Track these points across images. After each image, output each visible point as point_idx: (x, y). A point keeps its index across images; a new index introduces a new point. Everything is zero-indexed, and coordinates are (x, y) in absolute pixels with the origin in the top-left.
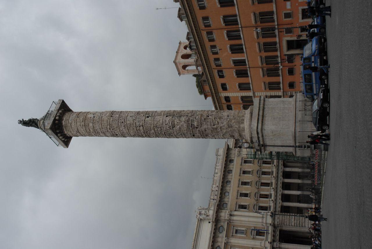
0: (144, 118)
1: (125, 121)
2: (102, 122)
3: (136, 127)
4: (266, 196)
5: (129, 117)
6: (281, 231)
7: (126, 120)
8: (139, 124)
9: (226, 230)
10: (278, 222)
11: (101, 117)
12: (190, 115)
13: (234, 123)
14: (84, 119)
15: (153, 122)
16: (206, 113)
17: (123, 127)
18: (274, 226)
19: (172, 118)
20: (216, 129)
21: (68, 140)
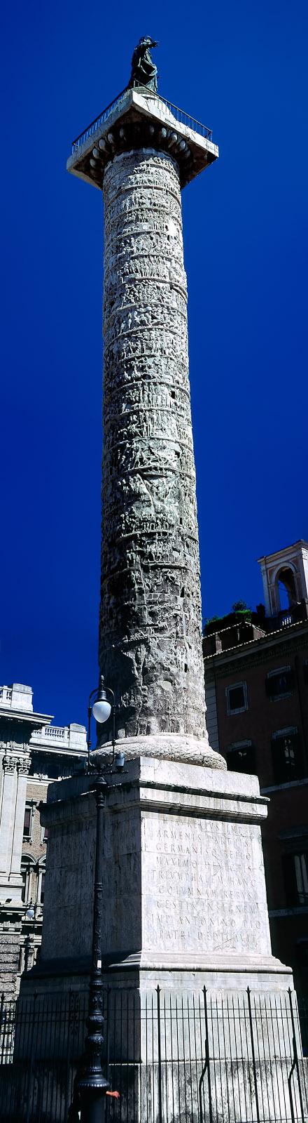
0: (171, 383)
1: (157, 324)
2: (152, 259)
3: (142, 356)
5: (172, 336)
7: (161, 327)
8: (150, 367)
11: (170, 257)
12: (185, 530)
13: (163, 690)
15: (157, 408)
16: (194, 590)
19: (174, 472)
20: (139, 622)
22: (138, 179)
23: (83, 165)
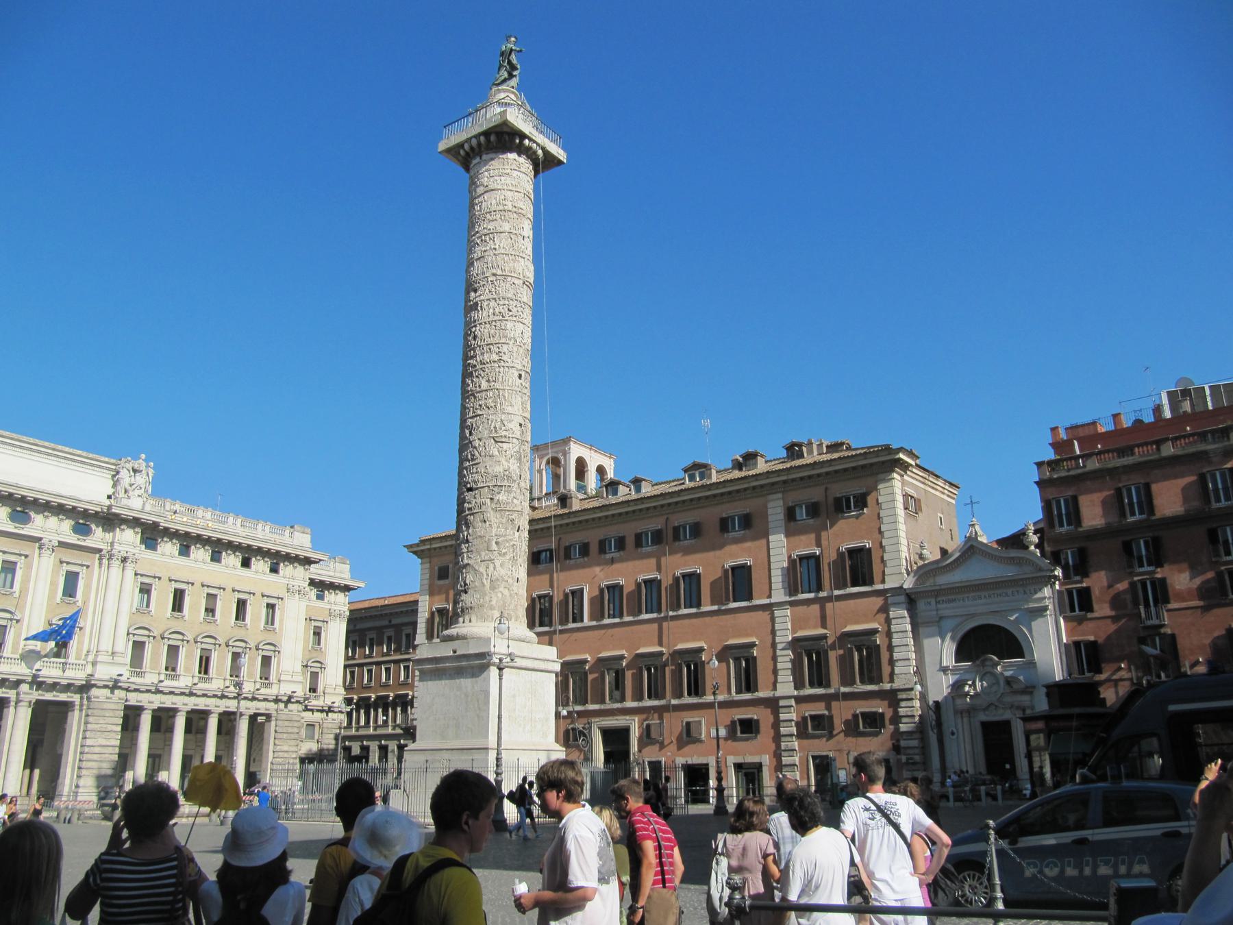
0: (519, 367)
4: (171, 667)
6: (66, 707)
7: (515, 319)
8: (504, 353)
9: (79, 543)
10: (98, 697)
11: (524, 256)
14: (520, 211)
17: (497, 311)
18: (85, 688)
21: (460, 158)
22: (503, 182)
23: (453, 151)
